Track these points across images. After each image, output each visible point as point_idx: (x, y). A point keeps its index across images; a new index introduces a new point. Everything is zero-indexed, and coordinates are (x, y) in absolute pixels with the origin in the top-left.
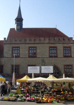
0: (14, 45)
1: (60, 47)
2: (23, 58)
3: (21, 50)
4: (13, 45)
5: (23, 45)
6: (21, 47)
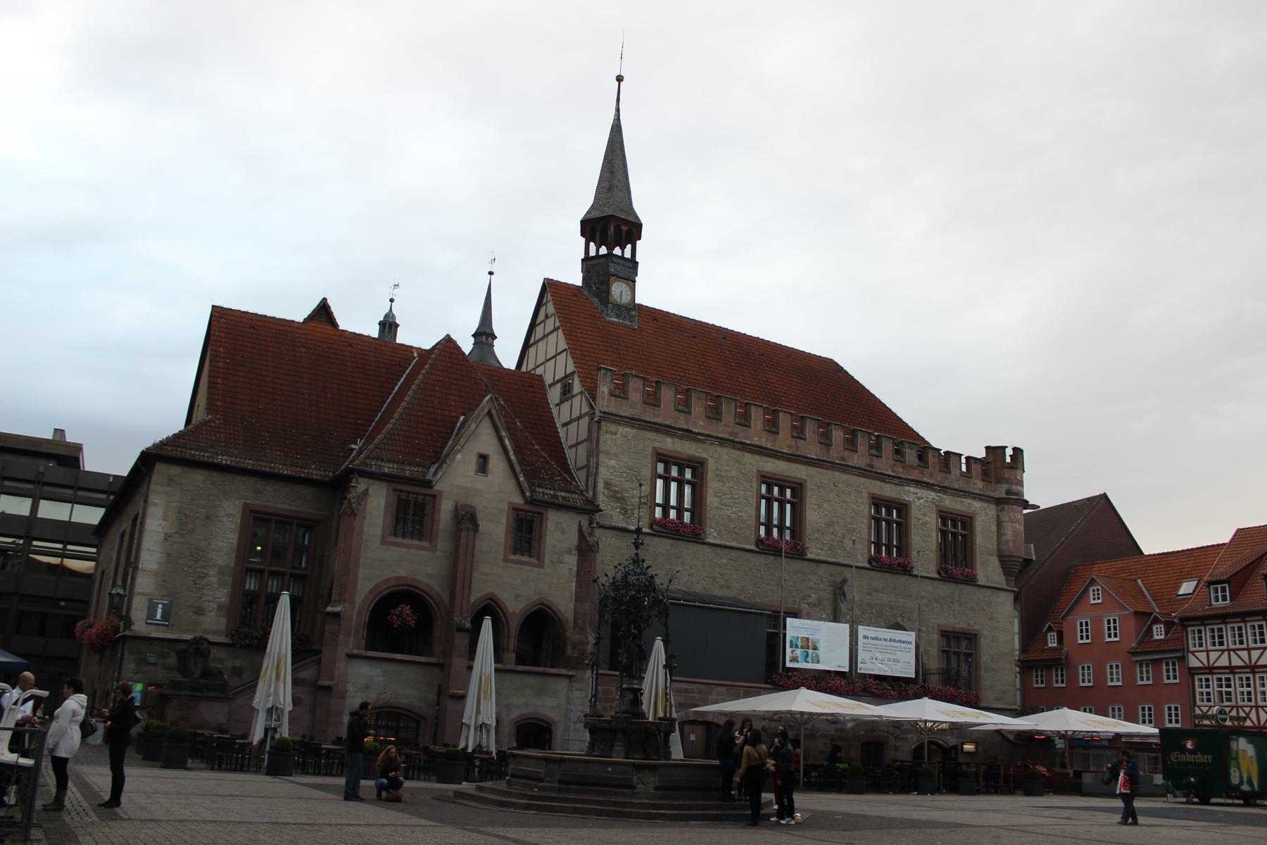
0: (670, 444)
1: (924, 506)
2: (727, 551)
3: (712, 485)
4: (661, 437)
5: (725, 453)
6: (711, 465)
